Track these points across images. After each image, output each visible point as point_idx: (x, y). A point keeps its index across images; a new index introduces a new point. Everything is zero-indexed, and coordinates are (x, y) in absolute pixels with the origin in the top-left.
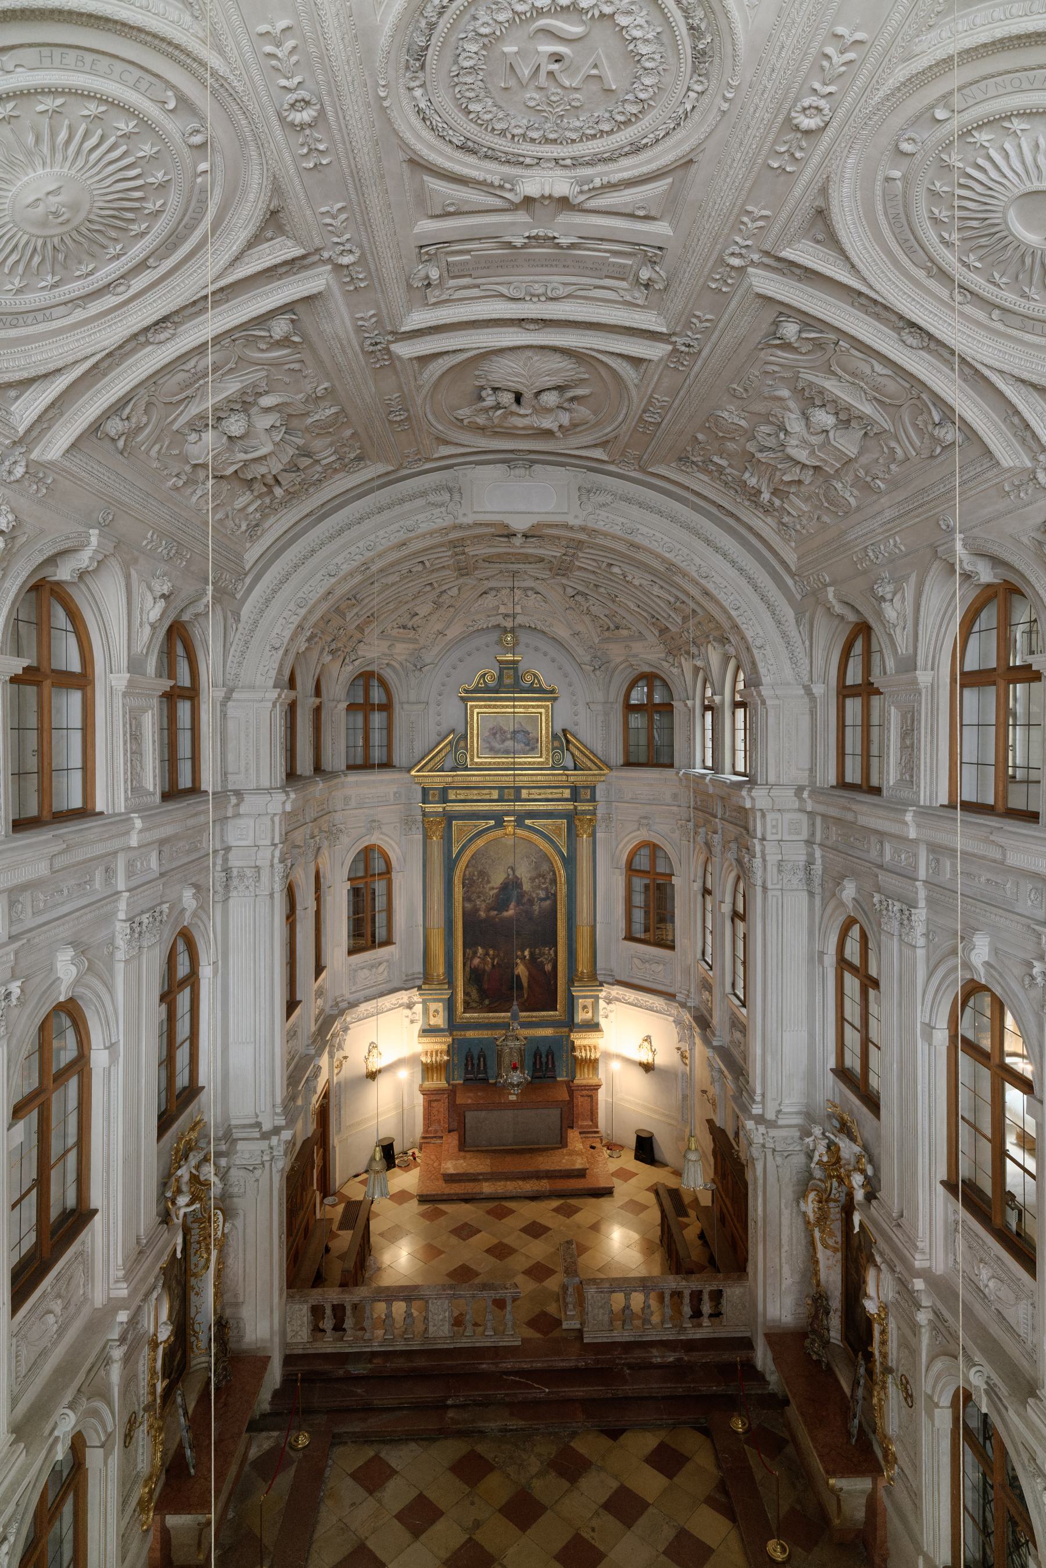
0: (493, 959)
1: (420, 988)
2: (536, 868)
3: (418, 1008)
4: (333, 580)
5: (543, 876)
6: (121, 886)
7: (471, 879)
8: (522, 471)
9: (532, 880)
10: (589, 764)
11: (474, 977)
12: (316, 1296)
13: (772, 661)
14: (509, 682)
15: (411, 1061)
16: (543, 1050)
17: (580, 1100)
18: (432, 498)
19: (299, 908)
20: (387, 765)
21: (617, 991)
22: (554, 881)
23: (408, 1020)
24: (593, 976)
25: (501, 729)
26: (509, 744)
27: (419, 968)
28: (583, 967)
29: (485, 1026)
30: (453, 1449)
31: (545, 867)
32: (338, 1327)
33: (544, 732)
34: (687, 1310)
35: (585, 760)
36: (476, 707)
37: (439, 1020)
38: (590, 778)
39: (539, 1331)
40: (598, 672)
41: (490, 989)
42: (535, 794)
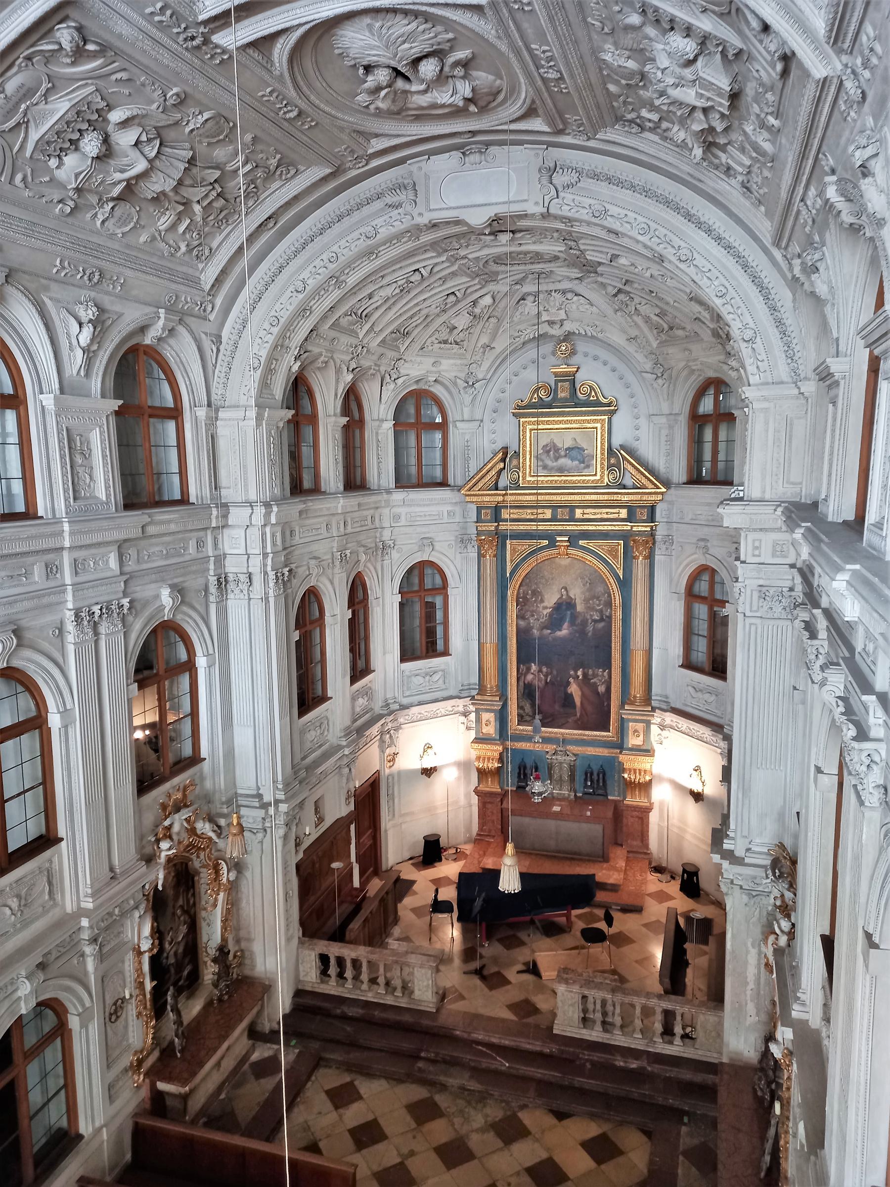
0: (546, 676)
1: (473, 698)
2: (590, 590)
3: (473, 716)
4: (301, 296)
5: (598, 598)
6: (68, 581)
7: (525, 598)
8: (475, 158)
9: (586, 601)
10: (644, 481)
11: (527, 692)
12: (323, 946)
13: (763, 356)
14: (564, 396)
15: (464, 766)
16: (595, 768)
17: (629, 821)
18: (389, 200)
19: (327, 614)
20: (443, 484)
21: (670, 718)
22: (609, 604)
23: (463, 727)
24: (647, 699)
25: (555, 445)
26: (563, 461)
27: (475, 680)
28: (637, 690)
29: (541, 741)
30: (417, 1092)
31: (600, 589)
32: (341, 975)
33: (598, 450)
34: (658, 1027)
35: (639, 476)
36: (529, 423)
37: (490, 730)
38: (645, 497)
39: (516, 1014)
40: (660, 381)
41: (546, 704)
42: (590, 513)
